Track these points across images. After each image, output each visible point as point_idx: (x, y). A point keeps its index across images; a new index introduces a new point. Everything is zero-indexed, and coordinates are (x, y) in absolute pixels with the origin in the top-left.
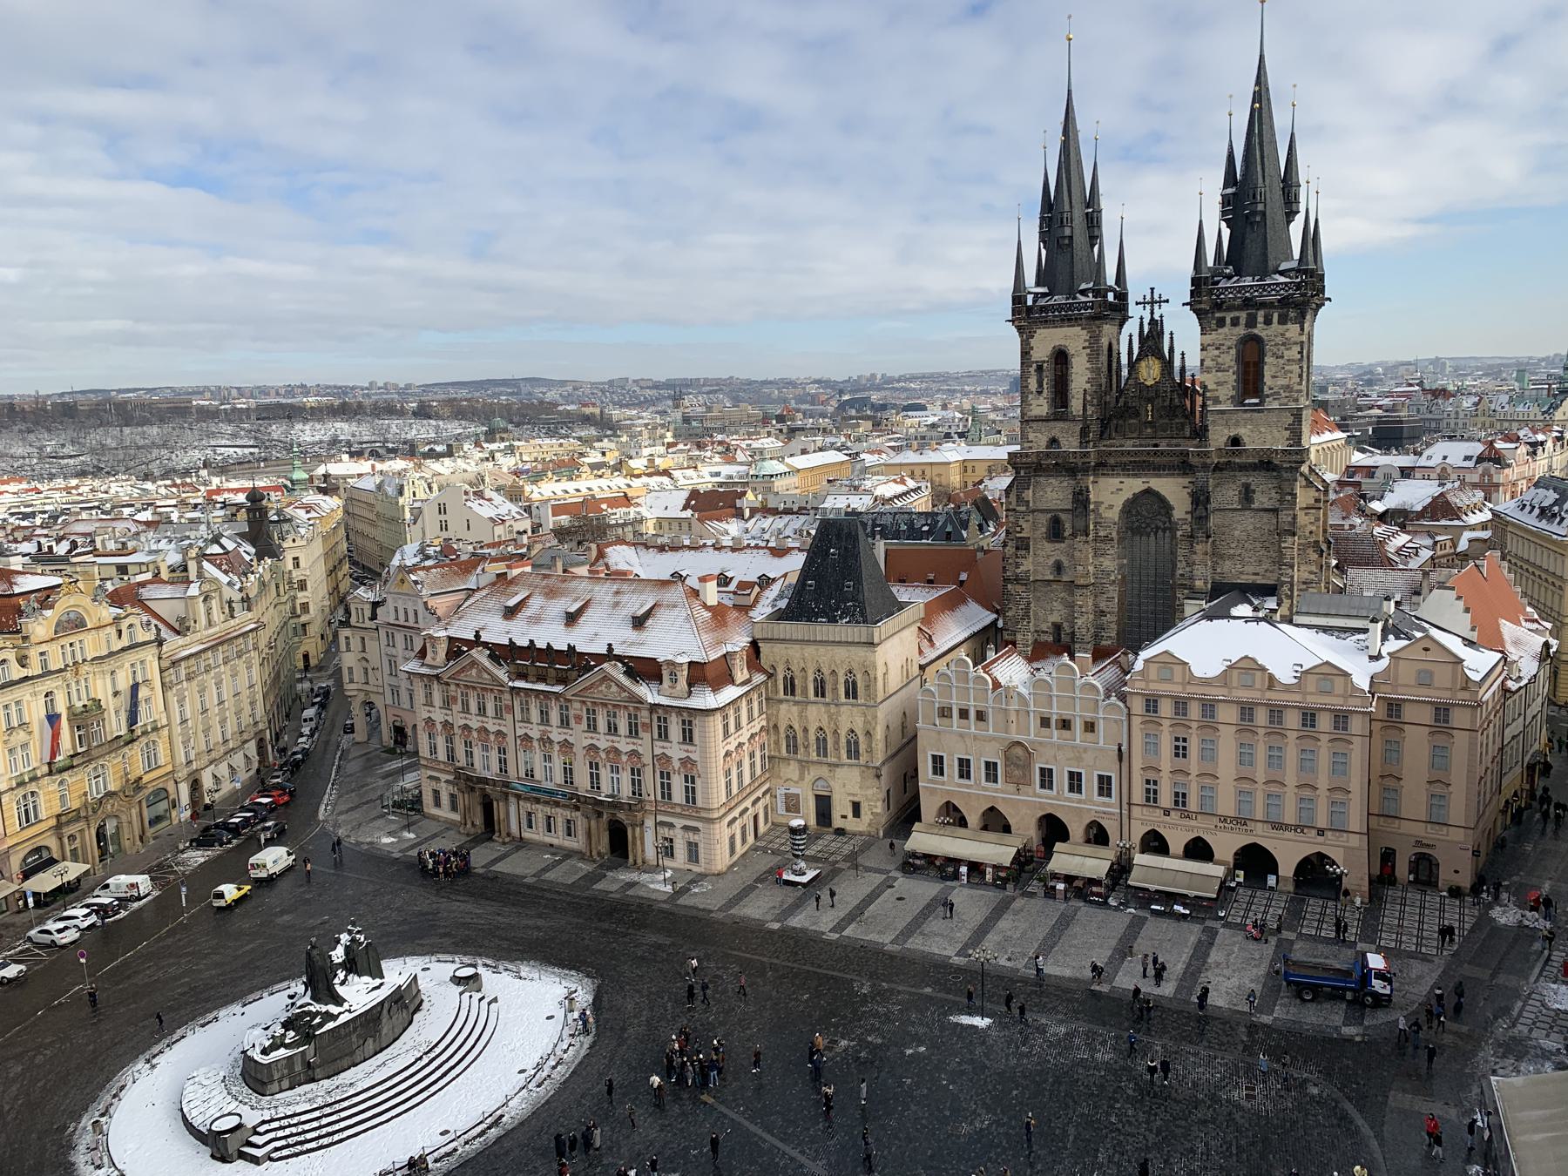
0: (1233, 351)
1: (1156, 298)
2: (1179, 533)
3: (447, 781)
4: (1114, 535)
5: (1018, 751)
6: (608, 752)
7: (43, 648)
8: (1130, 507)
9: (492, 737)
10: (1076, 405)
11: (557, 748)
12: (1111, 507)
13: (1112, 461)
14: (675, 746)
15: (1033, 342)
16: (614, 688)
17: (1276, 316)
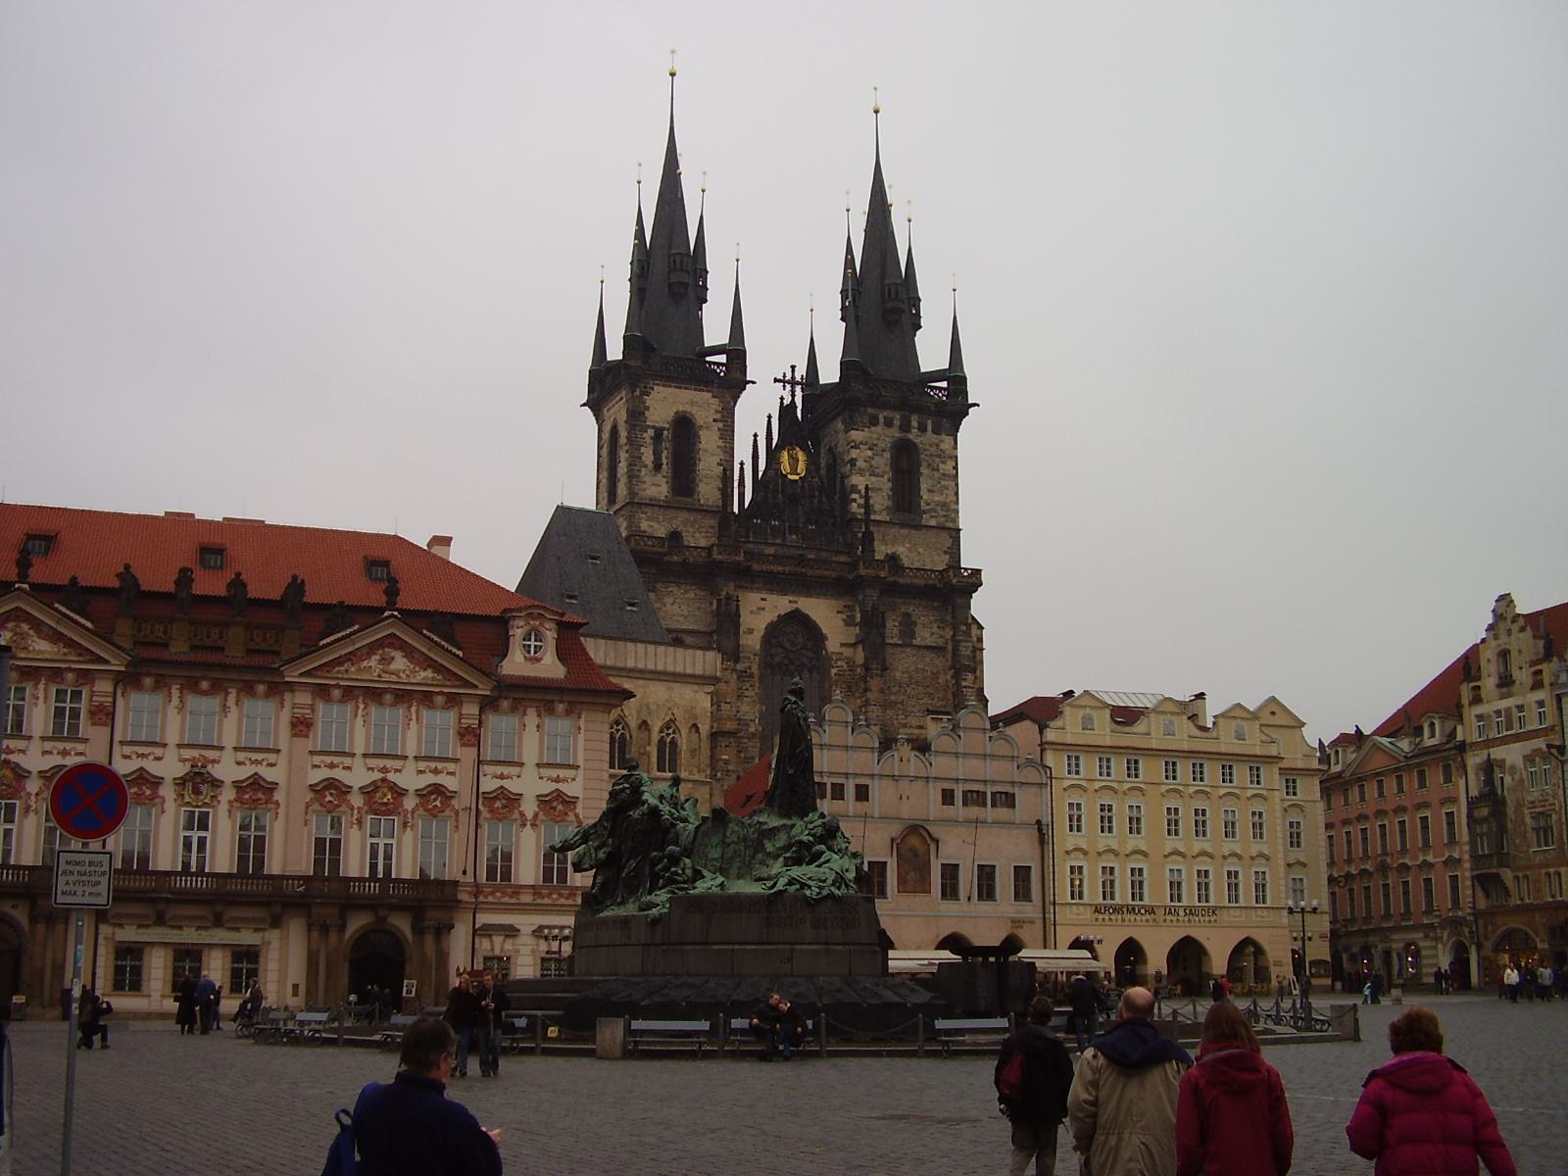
0: (887, 455)
1: (798, 379)
2: (834, 671)
4: (755, 669)
5: (914, 841)
6: (369, 792)
8: (773, 631)
9: (33, 786)
10: (707, 491)
11: (228, 794)
12: (750, 631)
13: (756, 567)
14: (530, 771)
15: (648, 401)
16: (400, 662)
17: (929, 422)
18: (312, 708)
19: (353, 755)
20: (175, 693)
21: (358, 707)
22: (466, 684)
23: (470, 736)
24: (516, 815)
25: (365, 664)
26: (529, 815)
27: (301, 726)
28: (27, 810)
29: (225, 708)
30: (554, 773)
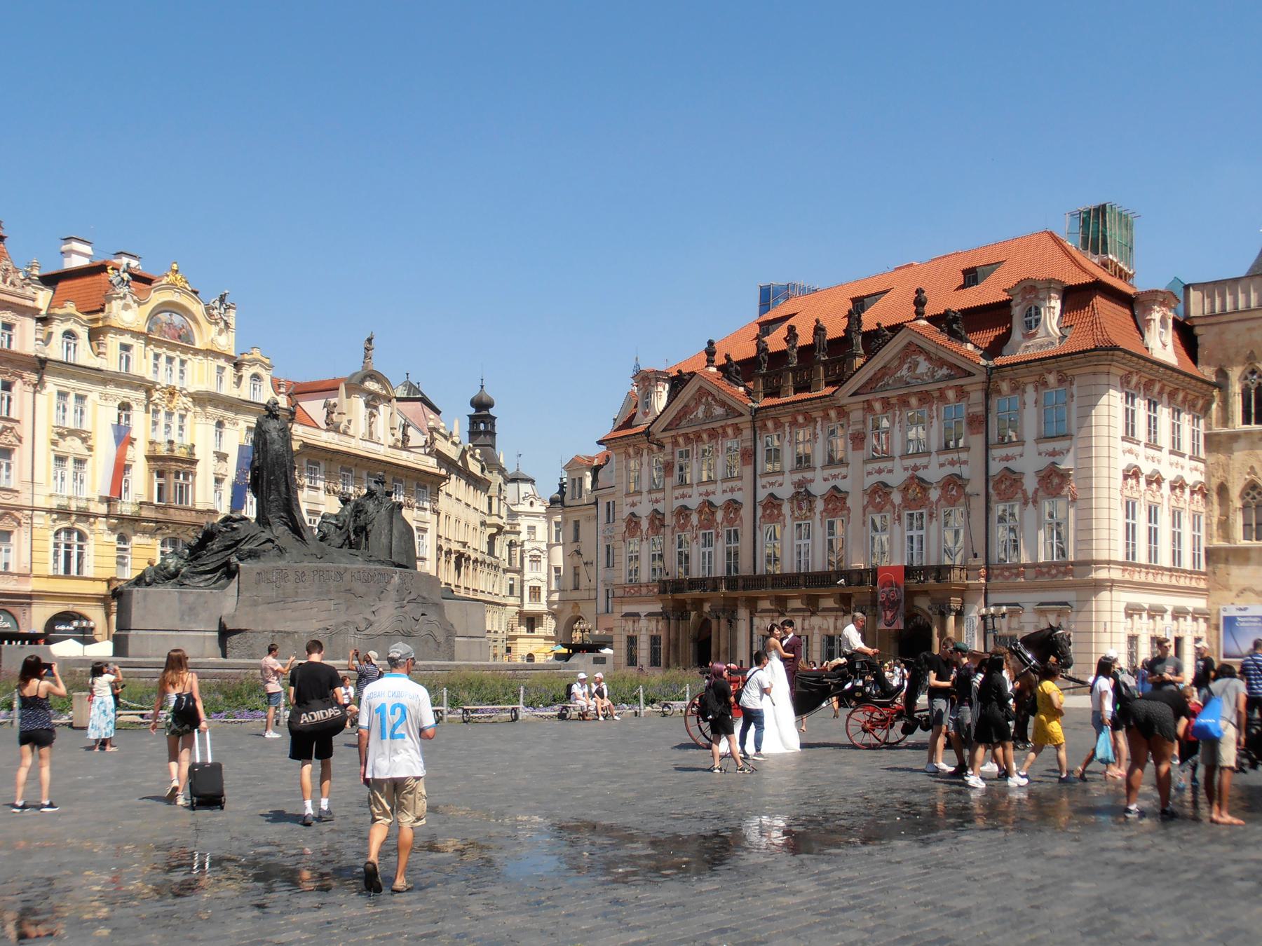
3: (650, 615)
7: (127, 339)
9: (719, 516)
11: (819, 505)
14: (1030, 448)
16: (924, 367)
18: (864, 422)
19: (892, 458)
20: (787, 429)
21: (894, 415)
22: (970, 374)
23: (979, 423)
24: (1020, 495)
25: (898, 374)
26: (1030, 494)
27: (858, 440)
28: (717, 536)
29: (815, 435)
30: (1049, 446)
